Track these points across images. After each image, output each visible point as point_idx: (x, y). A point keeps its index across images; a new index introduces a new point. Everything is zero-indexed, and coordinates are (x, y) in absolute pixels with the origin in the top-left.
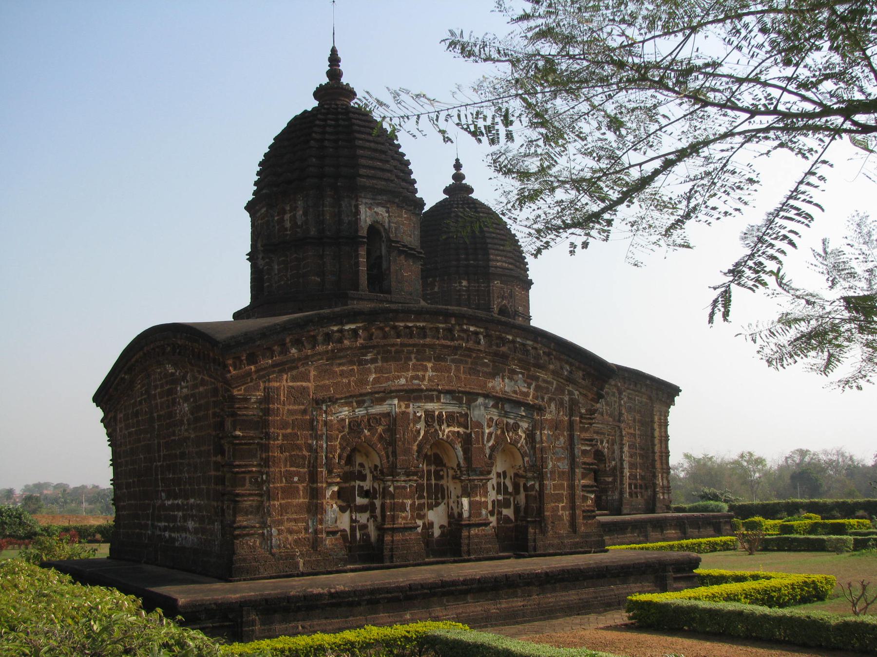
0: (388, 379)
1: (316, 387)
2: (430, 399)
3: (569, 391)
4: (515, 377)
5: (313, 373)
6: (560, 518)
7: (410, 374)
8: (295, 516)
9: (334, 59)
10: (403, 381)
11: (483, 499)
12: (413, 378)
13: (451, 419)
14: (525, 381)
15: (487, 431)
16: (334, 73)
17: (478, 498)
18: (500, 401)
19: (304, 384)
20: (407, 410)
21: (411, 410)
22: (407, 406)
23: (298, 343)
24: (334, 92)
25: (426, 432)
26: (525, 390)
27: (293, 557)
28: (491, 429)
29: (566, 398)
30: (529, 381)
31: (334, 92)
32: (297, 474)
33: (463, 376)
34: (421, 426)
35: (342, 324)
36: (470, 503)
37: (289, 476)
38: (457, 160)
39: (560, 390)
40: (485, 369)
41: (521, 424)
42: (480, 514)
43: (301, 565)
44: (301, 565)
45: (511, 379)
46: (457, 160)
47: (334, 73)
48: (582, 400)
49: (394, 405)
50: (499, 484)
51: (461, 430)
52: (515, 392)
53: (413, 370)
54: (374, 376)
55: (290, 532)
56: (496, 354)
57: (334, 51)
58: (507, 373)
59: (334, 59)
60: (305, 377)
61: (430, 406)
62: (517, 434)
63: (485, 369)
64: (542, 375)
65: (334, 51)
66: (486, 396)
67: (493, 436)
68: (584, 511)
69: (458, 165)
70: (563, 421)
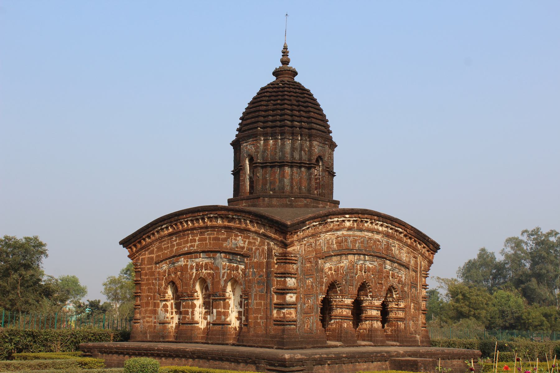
0: (181, 249)
1: (156, 256)
2: (196, 258)
3: (268, 243)
4: (238, 239)
5: (155, 250)
6: (259, 324)
7: (189, 245)
8: (149, 315)
9: (285, 52)
10: (186, 249)
11: (222, 310)
12: (191, 246)
13: (206, 266)
14: (242, 240)
15: (223, 271)
16: (285, 62)
17: (220, 310)
18: (232, 254)
19: (152, 255)
20: (188, 263)
21: (189, 263)
22: (187, 261)
23: (149, 237)
24: (285, 73)
25: (196, 274)
26: (242, 245)
27: (146, 333)
28: (225, 270)
29: (266, 248)
30: (244, 239)
31: (285, 73)
32: (150, 296)
33: (212, 242)
34: (194, 271)
35: (162, 226)
36: (217, 312)
37: (148, 296)
39: (262, 243)
40: (223, 236)
41: (239, 266)
42: (221, 318)
43: (148, 337)
44: (148, 337)
45: (235, 240)
47: (285, 62)
48: (276, 247)
49: (182, 262)
50: (241, 302)
51: (212, 271)
52: (237, 247)
53: (191, 243)
54: (176, 248)
55: (148, 322)
56: (226, 227)
57: (285, 48)
58: (233, 237)
59: (285, 52)
60: (152, 252)
61: (197, 260)
62: (238, 272)
63: (223, 236)
64: (251, 235)
65: (285, 48)
66: (221, 253)
67: (226, 275)
68: (275, 321)
70: (263, 263)
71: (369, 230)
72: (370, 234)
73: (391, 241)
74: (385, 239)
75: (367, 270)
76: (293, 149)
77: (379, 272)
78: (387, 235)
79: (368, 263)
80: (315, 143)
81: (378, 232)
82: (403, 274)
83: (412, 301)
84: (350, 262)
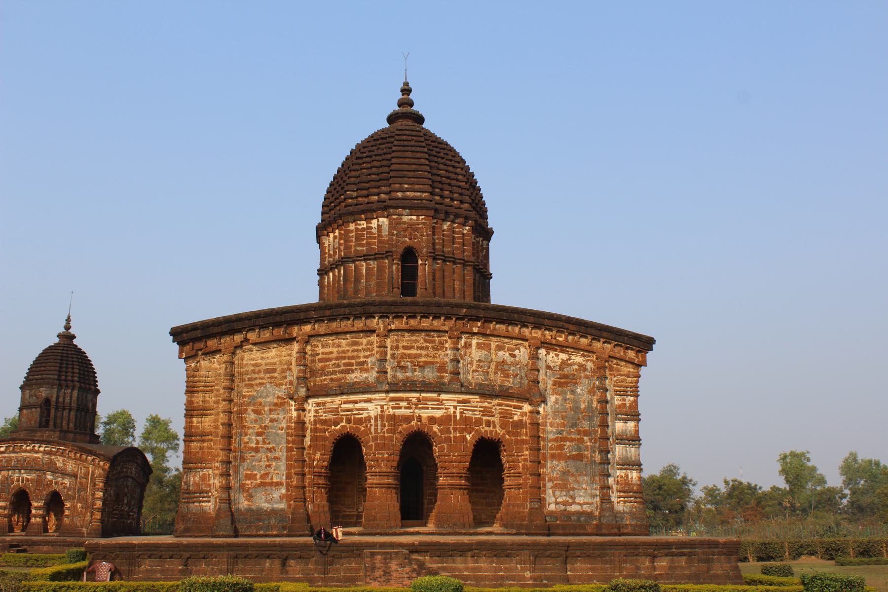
9: (68, 320)
16: (68, 327)
24: (67, 338)
31: (67, 338)
38: (406, 84)
46: (406, 84)
47: (68, 327)
57: (69, 317)
59: (68, 320)
65: (69, 317)
69: (406, 91)
71: (26, 451)
72: (28, 455)
73: (53, 457)
74: (46, 457)
75: (28, 480)
76: (31, 396)
77: (39, 482)
78: (49, 453)
79: (25, 476)
80: (41, 389)
81: (37, 452)
82: (67, 481)
83: (79, 501)
84: (4, 476)
